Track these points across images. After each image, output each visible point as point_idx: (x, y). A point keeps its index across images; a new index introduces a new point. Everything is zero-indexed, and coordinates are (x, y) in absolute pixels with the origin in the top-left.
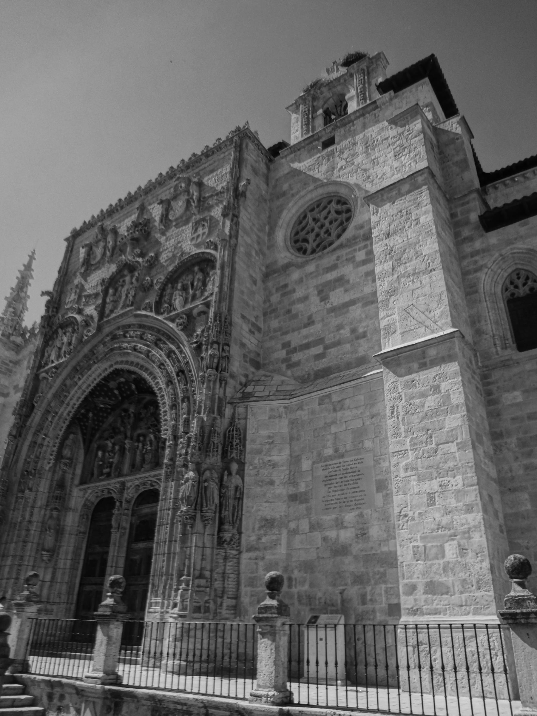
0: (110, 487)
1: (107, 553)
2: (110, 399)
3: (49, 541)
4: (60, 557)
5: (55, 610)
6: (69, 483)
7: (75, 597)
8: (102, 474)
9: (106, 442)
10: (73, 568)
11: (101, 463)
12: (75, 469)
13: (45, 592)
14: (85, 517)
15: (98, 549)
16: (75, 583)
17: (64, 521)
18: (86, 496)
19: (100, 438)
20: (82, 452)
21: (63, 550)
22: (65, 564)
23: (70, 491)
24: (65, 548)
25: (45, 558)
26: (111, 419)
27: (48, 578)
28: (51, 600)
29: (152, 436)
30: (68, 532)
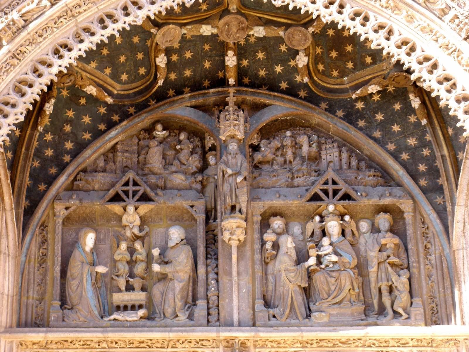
2: (115, 76)
8: (107, 309)
9: (117, 208)
11: (101, 269)
19: (71, 188)
26: (114, 136)
29: (333, 226)
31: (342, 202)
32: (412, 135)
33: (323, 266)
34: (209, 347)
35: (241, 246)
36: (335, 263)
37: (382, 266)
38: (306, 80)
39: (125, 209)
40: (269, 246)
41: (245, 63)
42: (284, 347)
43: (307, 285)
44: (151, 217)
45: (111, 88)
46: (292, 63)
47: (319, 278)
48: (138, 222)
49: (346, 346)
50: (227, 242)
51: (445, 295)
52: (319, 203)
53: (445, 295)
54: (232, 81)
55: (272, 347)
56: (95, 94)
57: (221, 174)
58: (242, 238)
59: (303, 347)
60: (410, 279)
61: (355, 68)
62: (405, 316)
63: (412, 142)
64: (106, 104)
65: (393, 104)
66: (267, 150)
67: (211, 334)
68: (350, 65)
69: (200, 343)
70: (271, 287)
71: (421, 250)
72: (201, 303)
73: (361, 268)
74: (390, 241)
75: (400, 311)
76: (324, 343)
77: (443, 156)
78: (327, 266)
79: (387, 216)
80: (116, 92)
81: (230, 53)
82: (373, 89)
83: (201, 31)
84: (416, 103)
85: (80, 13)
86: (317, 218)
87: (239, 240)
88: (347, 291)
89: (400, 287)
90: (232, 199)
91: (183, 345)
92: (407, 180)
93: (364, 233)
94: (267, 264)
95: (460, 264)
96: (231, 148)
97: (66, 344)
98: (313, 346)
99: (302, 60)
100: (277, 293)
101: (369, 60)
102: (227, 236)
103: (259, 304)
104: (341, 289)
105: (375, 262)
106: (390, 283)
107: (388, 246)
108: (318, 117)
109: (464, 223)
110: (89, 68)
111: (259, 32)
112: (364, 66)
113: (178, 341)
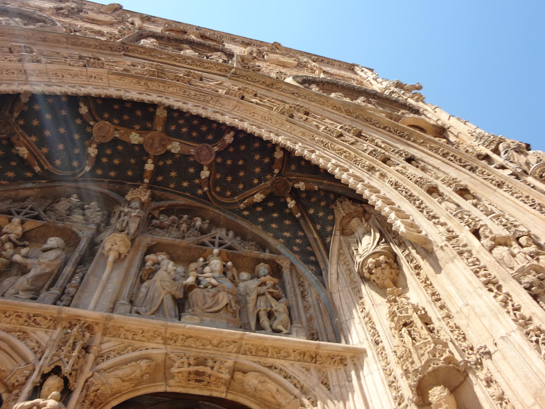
29: (216, 263)
31: (226, 250)
32: (287, 231)
33: (201, 286)
34: (43, 326)
35: (119, 259)
36: (214, 286)
37: (262, 298)
38: (206, 189)
39: (10, 221)
40: (149, 263)
41: (160, 178)
42: (141, 341)
43: (181, 296)
44: (36, 237)
45: (43, 163)
46: (197, 181)
47: (196, 294)
48: (19, 230)
49: (217, 348)
50: (106, 254)
51: (325, 327)
52: (205, 248)
53: (325, 327)
54: (146, 181)
55: (126, 338)
56: (26, 156)
57: (119, 213)
58: (123, 250)
59: (164, 344)
60: (289, 308)
61: (244, 189)
62: (285, 331)
63: (287, 234)
64: (33, 171)
65: (273, 214)
66: (165, 220)
67: (53, 310)
68: (241, 186)
69: (32, 319)
70: (141, 295)
71: (298, 292)
72: (55, 291)
73: (240, 300)
74: (270, 281)
75: (280, 327)
76: (189, 342)
77: (315, 239)
78: (206, 287)
79: (266, 265)
80: (46, 168)
81: (150, 161)
82: (258, 197)
83: (131, 137)
84: (291, 204)
85: (32, 75)
86: (201, 259)
87: (120, 255)
88: (225, 304)
89: (281, 310)
90: (122, 225)
91: (8, 320)
92: (283, 250)
93: (244, 281)
94: (142, 281)
95: (337, 303)
96: (133, 204)
98: (177, 343)
99: (205, 174)
100: (148, 297)
101: (256, 181)
102: (108, 246)
103: (124, 301)
104: (217, 303)
105: (253, 296)
106: (269, 309)
107: (267, 282)
108: (213, 211)
109: (338, 274)
110: (29, 139)
111: (175, 147)
112: (252, 186)
113: (5, 313)
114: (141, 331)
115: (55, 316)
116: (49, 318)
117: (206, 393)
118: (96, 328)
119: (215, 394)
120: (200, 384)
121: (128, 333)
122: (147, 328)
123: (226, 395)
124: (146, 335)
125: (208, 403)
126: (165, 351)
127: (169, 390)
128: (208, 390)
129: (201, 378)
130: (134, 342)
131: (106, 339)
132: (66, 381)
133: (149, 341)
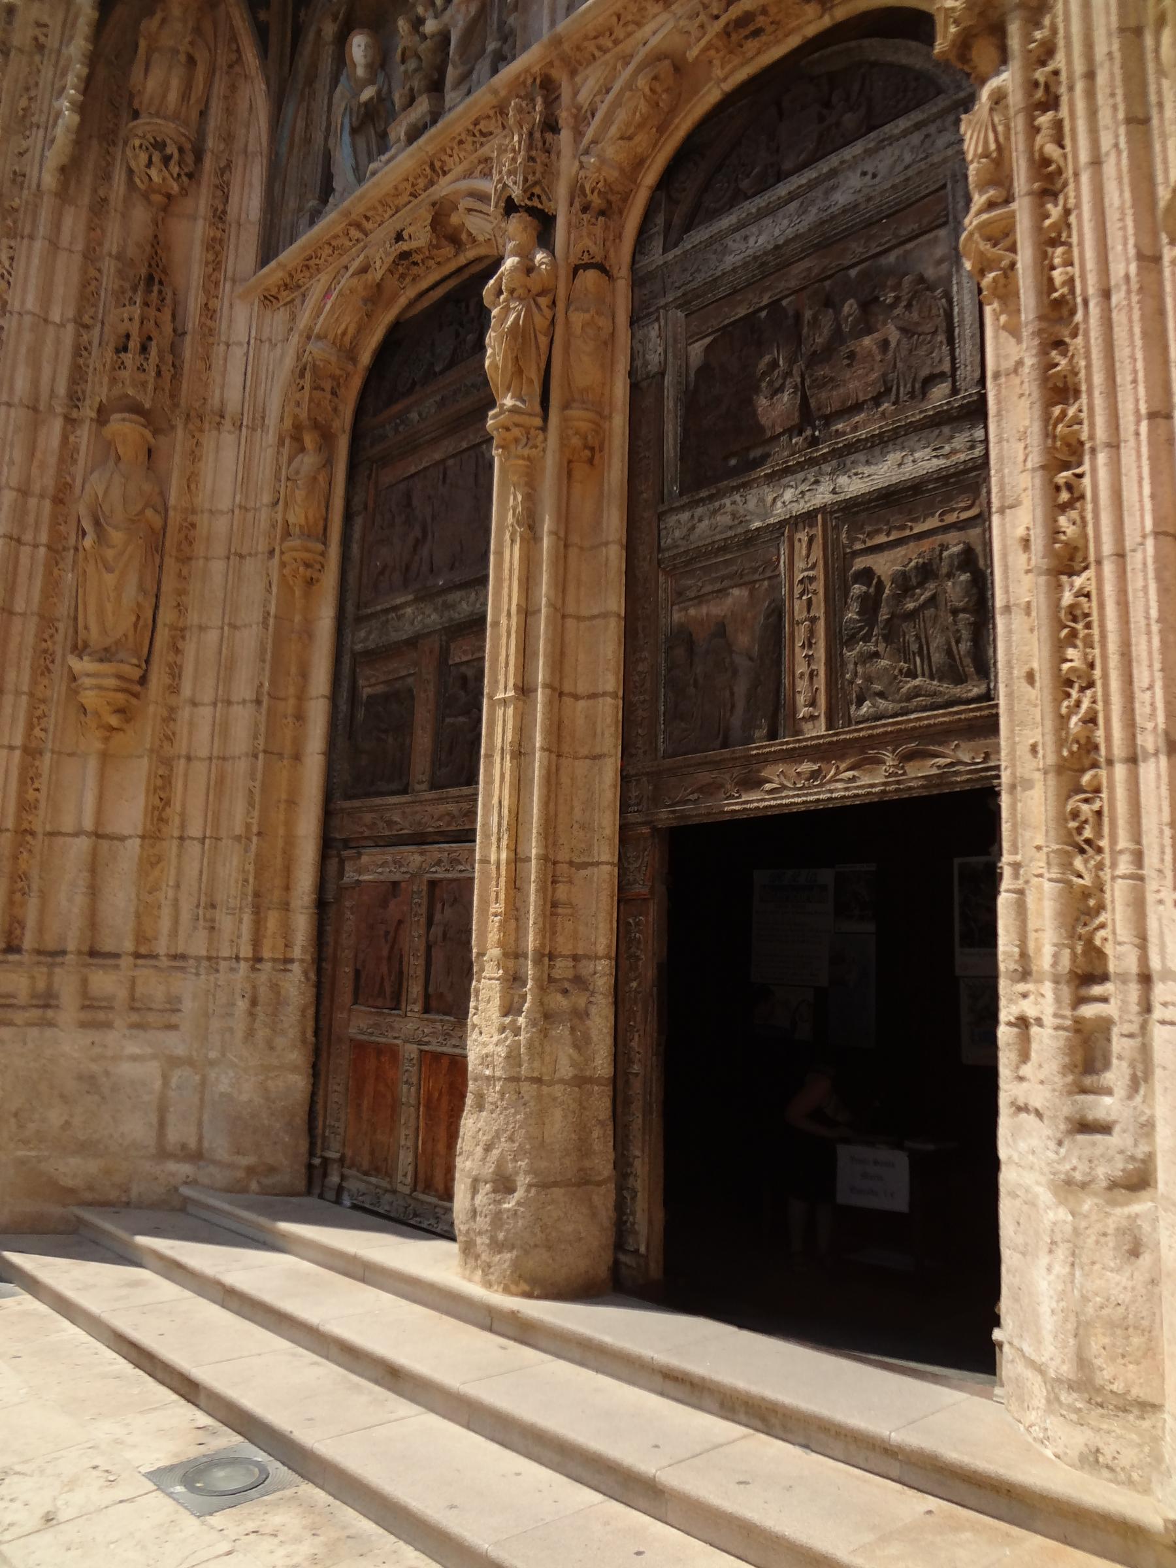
0: (444, 187)
1: (476, 624)
3: (110, 596)
4: (187, 690)
5: (188, 1005)
6: (196, 273)
7: (302, 924)
10: (275, 751)
12: (223, 191)
13: (120, 900)
14: (309, 440)
15: (418, 618)
16: (290, 842)
17: (191, 480)
18: (304, 320)
20: (255, 95)
21: (202, 649)
22: (222, 730)
23: (209, 312)
24: (212, 636)
25: (89, 698)
27: (129, 815)
28: (162, 947)
30: (219, 549)
97: (312, 263)
114: (615, 19)
115: (495, 102)
116: (491, 113)
117: (794, 42)
118: (555, 73)
119: (811, 31)
120: (764, 38)
121: (601, 41)
122: (619, 5)
123: (832, 17)
124: (630, 18)
125: (816, 55)
126: (671, 25)
127: (728, 86)
128: (787, 36)
129: (751, 28)
130: (620, 47)
131: (578, 79)
132: (531, 211)
133: (639, 24)
